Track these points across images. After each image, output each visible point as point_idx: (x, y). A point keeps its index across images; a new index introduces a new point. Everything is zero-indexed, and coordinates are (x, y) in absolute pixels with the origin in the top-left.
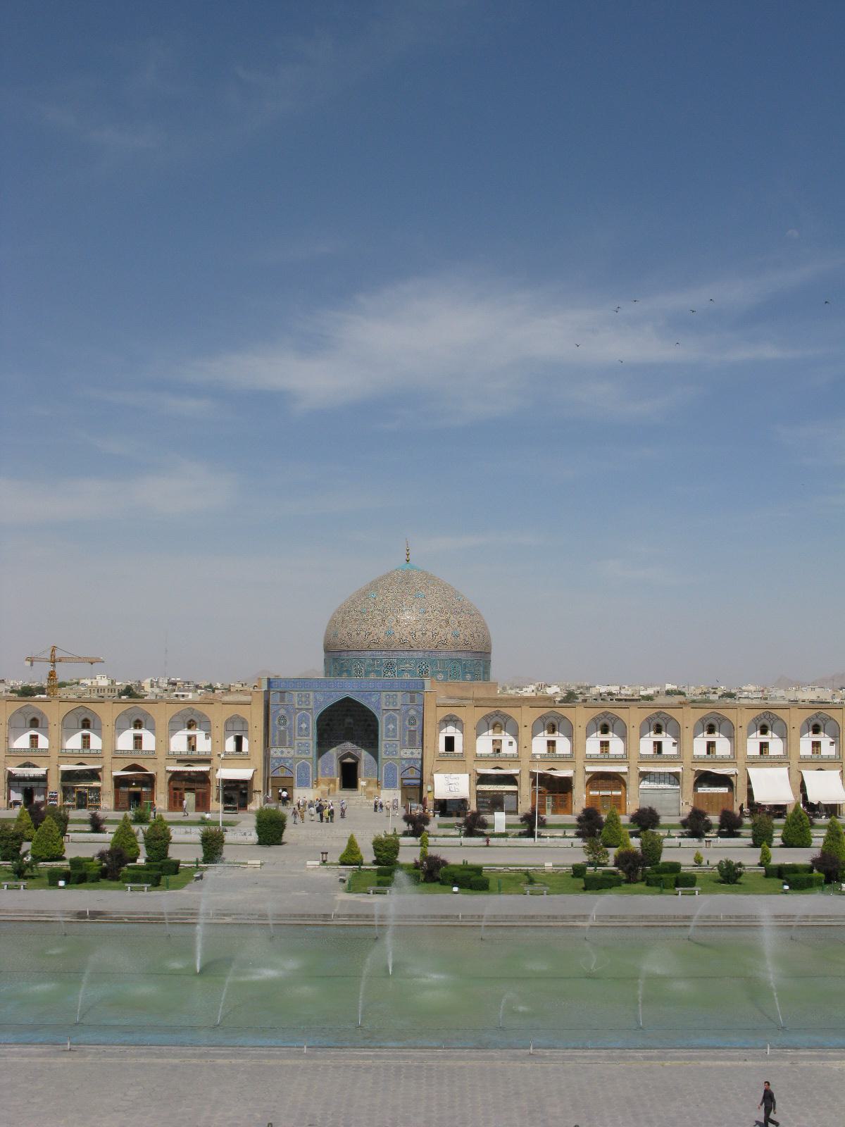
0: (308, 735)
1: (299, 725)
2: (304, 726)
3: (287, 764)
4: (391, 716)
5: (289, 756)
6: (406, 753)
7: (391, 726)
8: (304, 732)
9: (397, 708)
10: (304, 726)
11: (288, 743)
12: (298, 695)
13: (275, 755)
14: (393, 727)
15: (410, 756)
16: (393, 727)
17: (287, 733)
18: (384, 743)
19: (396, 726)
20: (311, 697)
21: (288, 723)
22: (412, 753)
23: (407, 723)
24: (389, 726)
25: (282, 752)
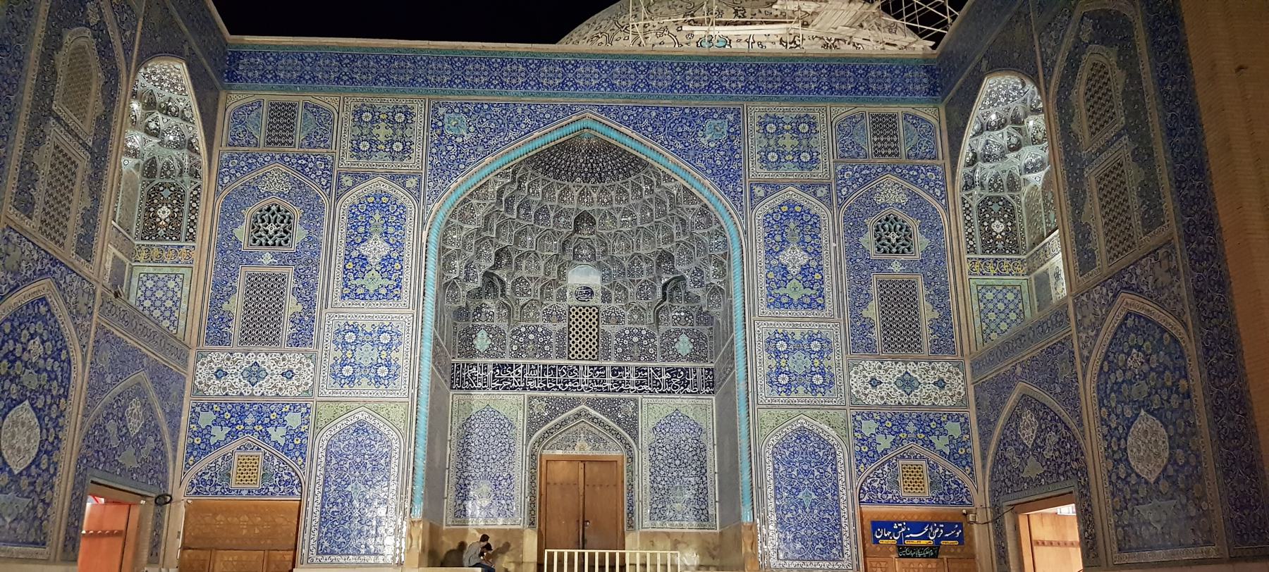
0: (392, 293)
1: (351, 244)
2: (375, 248)
3: (277, 434)
4: (791, 211)
5: (291, 390)
6: (875, 383)
7: (794, 257)
8: (374, 280)
9: (819, 173)
10: (375, 248)
11: (287, 329)
12: (358, 113)
13: (215, 389)
14: (803, 259)
15: (899, 396)
16: (803, 259)
17: (291, 283)
18: (764, 330)
19: (817, 253)
20: (419, 121)
21: (299, 234)
22: (907, 383)
23: (868, 240)
24: (786, 257)
25: (255, 373)
